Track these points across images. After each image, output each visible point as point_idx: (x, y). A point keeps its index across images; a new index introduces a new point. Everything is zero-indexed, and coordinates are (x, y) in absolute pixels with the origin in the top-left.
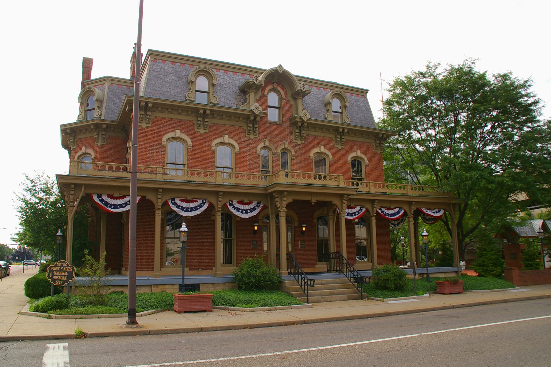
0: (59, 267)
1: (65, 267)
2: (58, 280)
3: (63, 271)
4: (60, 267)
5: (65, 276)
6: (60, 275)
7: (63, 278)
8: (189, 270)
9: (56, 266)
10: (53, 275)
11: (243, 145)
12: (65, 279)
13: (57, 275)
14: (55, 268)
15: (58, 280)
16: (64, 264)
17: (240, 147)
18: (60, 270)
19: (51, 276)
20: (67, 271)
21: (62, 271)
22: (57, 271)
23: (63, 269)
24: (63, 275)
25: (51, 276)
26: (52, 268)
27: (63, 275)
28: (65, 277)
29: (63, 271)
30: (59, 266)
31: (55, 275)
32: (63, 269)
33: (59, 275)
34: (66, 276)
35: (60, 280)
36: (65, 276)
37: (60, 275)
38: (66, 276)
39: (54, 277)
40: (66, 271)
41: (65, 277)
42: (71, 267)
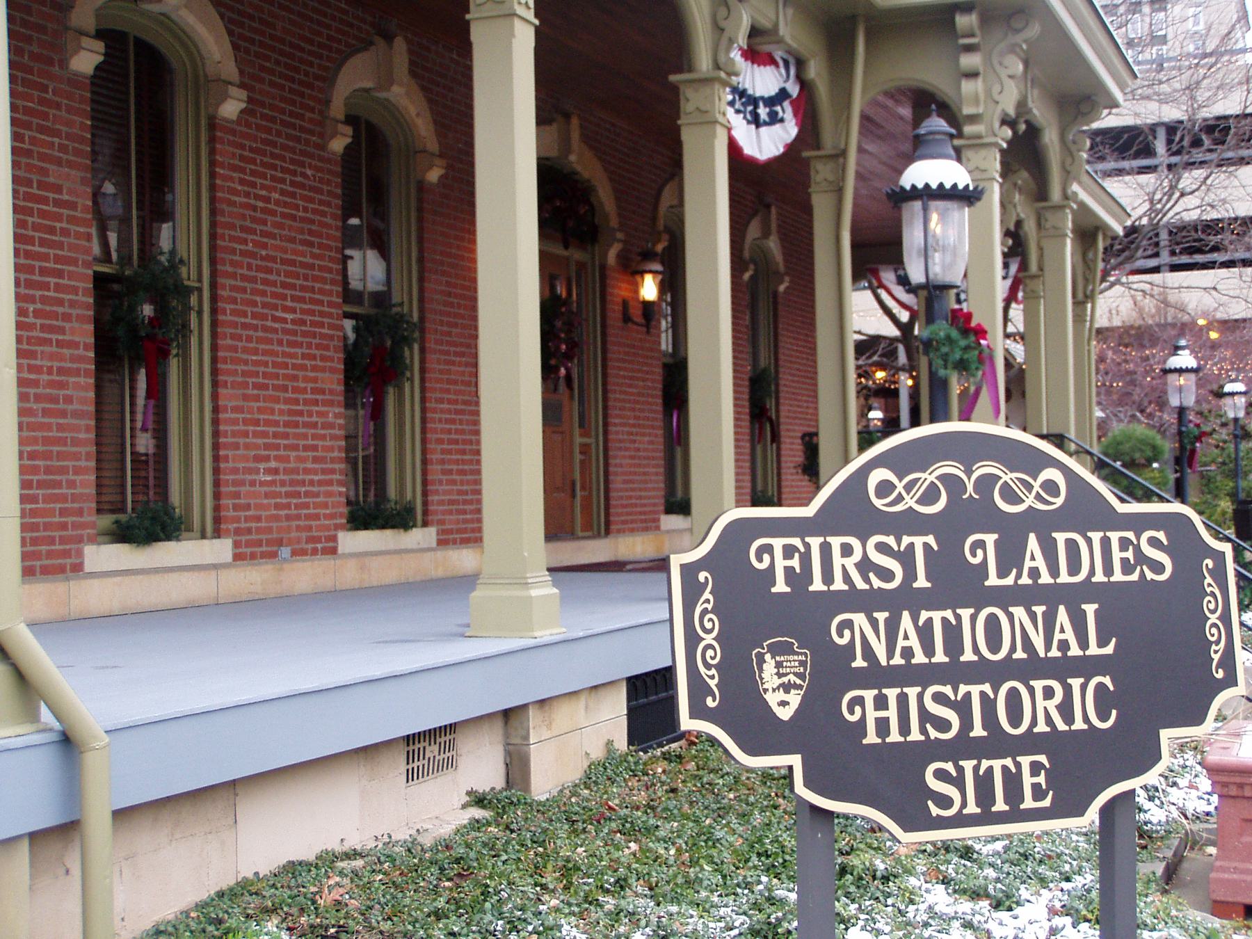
0: (919, 541)
1: (1043, 524)
2: (963, 747)
3: (1025, 596)
5: (1063, 668)
6: (982, 671)
8: (237, 557)
12: (1086, 714)
13: (925, 675)
15: (963, 747)
16: (1008, 477)
20: (1088, 590)
21: (1005, 597)
22: (907, 599)
23: (1010, 557)
24: (1033, 667)
27: (1033, 667)
29: (1025, 596)
30: (910, 523)
31: (877, 676)
32: (1010, 557)
33: (955, 672)
34: (1087, 667)
35: (997, 744)
36: (1063, 668)
37: (982, 671)
38: (1087, 667)
40: (1072, 597)
42: (1139, 523)
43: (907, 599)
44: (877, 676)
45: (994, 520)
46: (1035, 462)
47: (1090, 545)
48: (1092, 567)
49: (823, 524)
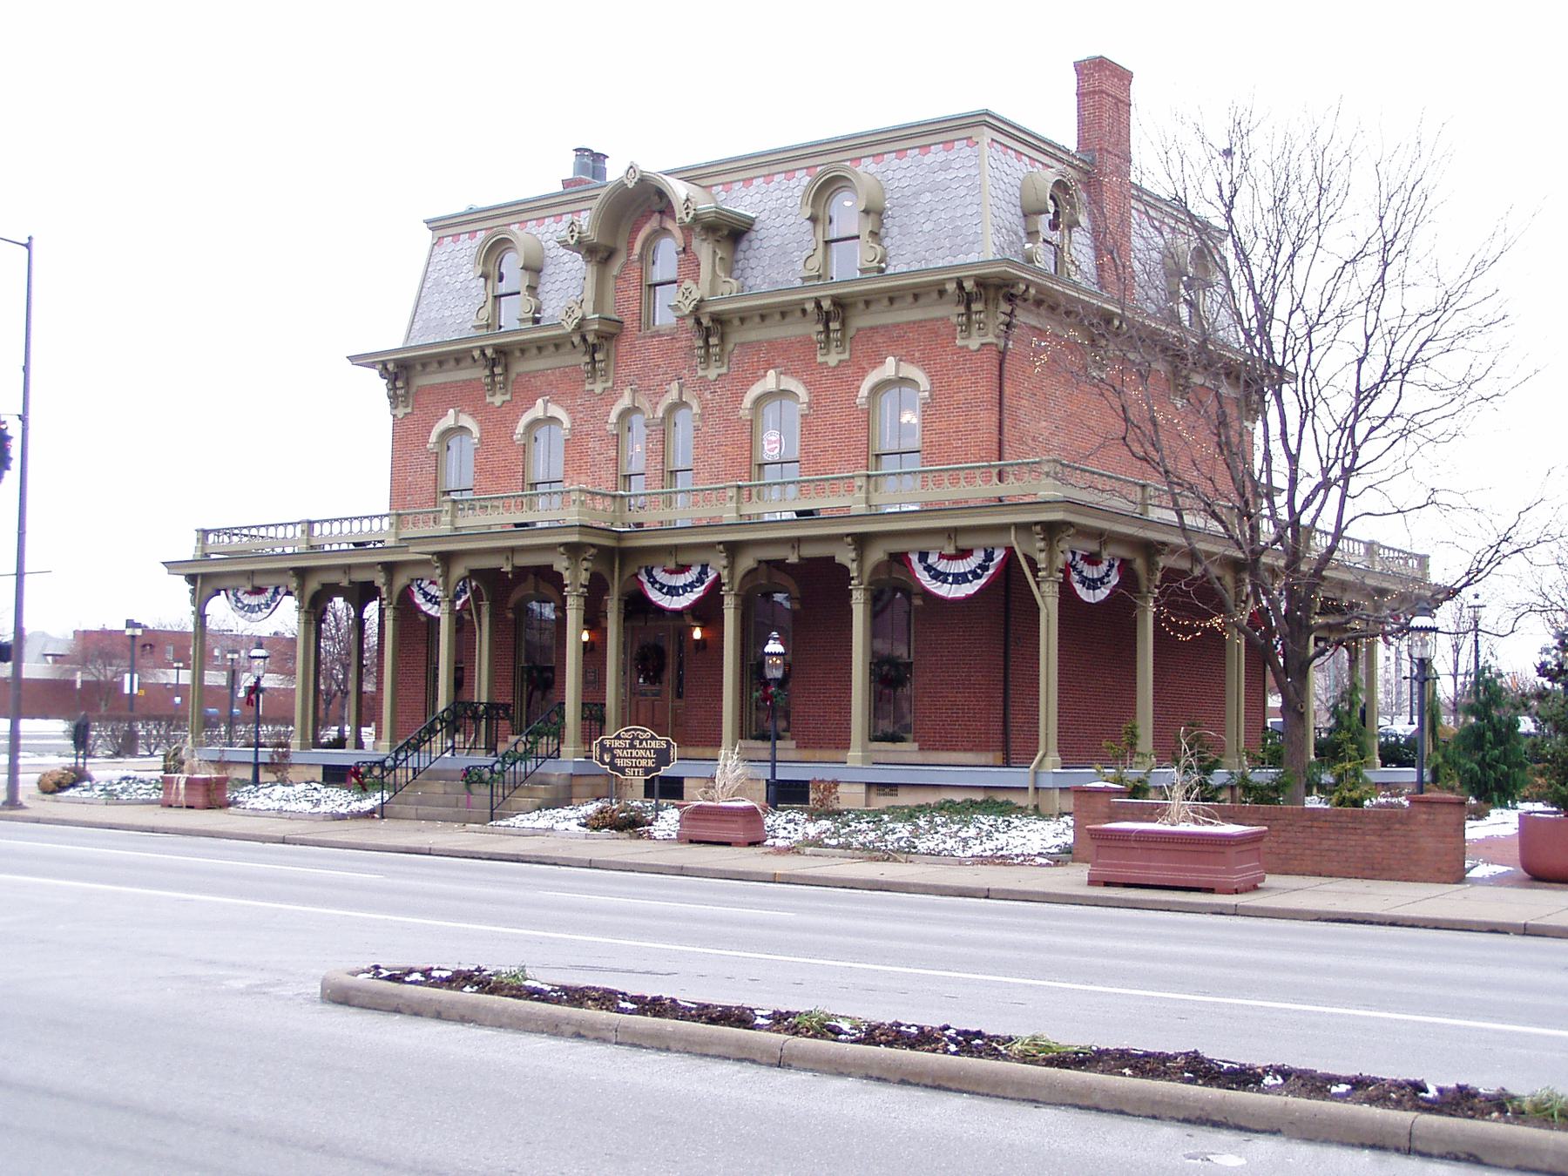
1: (646, 740)
4: (632, 740)
5: (648, 758)
7: (643, 763)
9: (618, 737)
10: (614, 757)
11: (581, 415)
14: (617, 743)
15: (631, 767)
17: (573, 421)
18: (632, 746)
19: (607, 760)
22: (625, 748)
23: (641, 744)
24: (643, 758)
25: (607, 760)
26: (607, 743)
27: (643, 758)
28: (650, 762)
31: (620, 757)
35: (636, 767)
36: (648, 758)
39: (618, 762)
40: (650, 749)
41: (650, 762)
43: (625, 748)
44: (620, 757)
45: (638, 739)
46: (645, 732)
47: (653, 743)
48: (653, 745)
49: (614, 739)
